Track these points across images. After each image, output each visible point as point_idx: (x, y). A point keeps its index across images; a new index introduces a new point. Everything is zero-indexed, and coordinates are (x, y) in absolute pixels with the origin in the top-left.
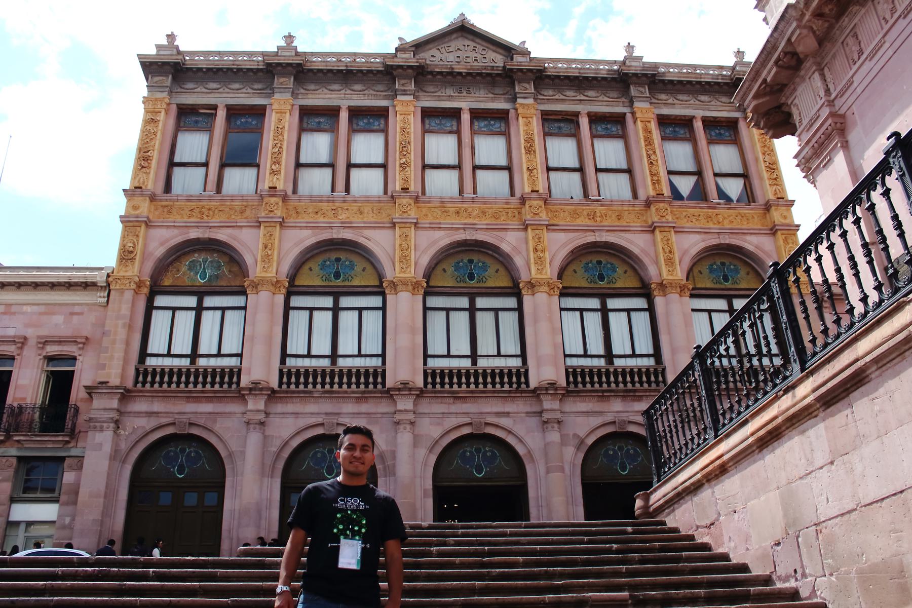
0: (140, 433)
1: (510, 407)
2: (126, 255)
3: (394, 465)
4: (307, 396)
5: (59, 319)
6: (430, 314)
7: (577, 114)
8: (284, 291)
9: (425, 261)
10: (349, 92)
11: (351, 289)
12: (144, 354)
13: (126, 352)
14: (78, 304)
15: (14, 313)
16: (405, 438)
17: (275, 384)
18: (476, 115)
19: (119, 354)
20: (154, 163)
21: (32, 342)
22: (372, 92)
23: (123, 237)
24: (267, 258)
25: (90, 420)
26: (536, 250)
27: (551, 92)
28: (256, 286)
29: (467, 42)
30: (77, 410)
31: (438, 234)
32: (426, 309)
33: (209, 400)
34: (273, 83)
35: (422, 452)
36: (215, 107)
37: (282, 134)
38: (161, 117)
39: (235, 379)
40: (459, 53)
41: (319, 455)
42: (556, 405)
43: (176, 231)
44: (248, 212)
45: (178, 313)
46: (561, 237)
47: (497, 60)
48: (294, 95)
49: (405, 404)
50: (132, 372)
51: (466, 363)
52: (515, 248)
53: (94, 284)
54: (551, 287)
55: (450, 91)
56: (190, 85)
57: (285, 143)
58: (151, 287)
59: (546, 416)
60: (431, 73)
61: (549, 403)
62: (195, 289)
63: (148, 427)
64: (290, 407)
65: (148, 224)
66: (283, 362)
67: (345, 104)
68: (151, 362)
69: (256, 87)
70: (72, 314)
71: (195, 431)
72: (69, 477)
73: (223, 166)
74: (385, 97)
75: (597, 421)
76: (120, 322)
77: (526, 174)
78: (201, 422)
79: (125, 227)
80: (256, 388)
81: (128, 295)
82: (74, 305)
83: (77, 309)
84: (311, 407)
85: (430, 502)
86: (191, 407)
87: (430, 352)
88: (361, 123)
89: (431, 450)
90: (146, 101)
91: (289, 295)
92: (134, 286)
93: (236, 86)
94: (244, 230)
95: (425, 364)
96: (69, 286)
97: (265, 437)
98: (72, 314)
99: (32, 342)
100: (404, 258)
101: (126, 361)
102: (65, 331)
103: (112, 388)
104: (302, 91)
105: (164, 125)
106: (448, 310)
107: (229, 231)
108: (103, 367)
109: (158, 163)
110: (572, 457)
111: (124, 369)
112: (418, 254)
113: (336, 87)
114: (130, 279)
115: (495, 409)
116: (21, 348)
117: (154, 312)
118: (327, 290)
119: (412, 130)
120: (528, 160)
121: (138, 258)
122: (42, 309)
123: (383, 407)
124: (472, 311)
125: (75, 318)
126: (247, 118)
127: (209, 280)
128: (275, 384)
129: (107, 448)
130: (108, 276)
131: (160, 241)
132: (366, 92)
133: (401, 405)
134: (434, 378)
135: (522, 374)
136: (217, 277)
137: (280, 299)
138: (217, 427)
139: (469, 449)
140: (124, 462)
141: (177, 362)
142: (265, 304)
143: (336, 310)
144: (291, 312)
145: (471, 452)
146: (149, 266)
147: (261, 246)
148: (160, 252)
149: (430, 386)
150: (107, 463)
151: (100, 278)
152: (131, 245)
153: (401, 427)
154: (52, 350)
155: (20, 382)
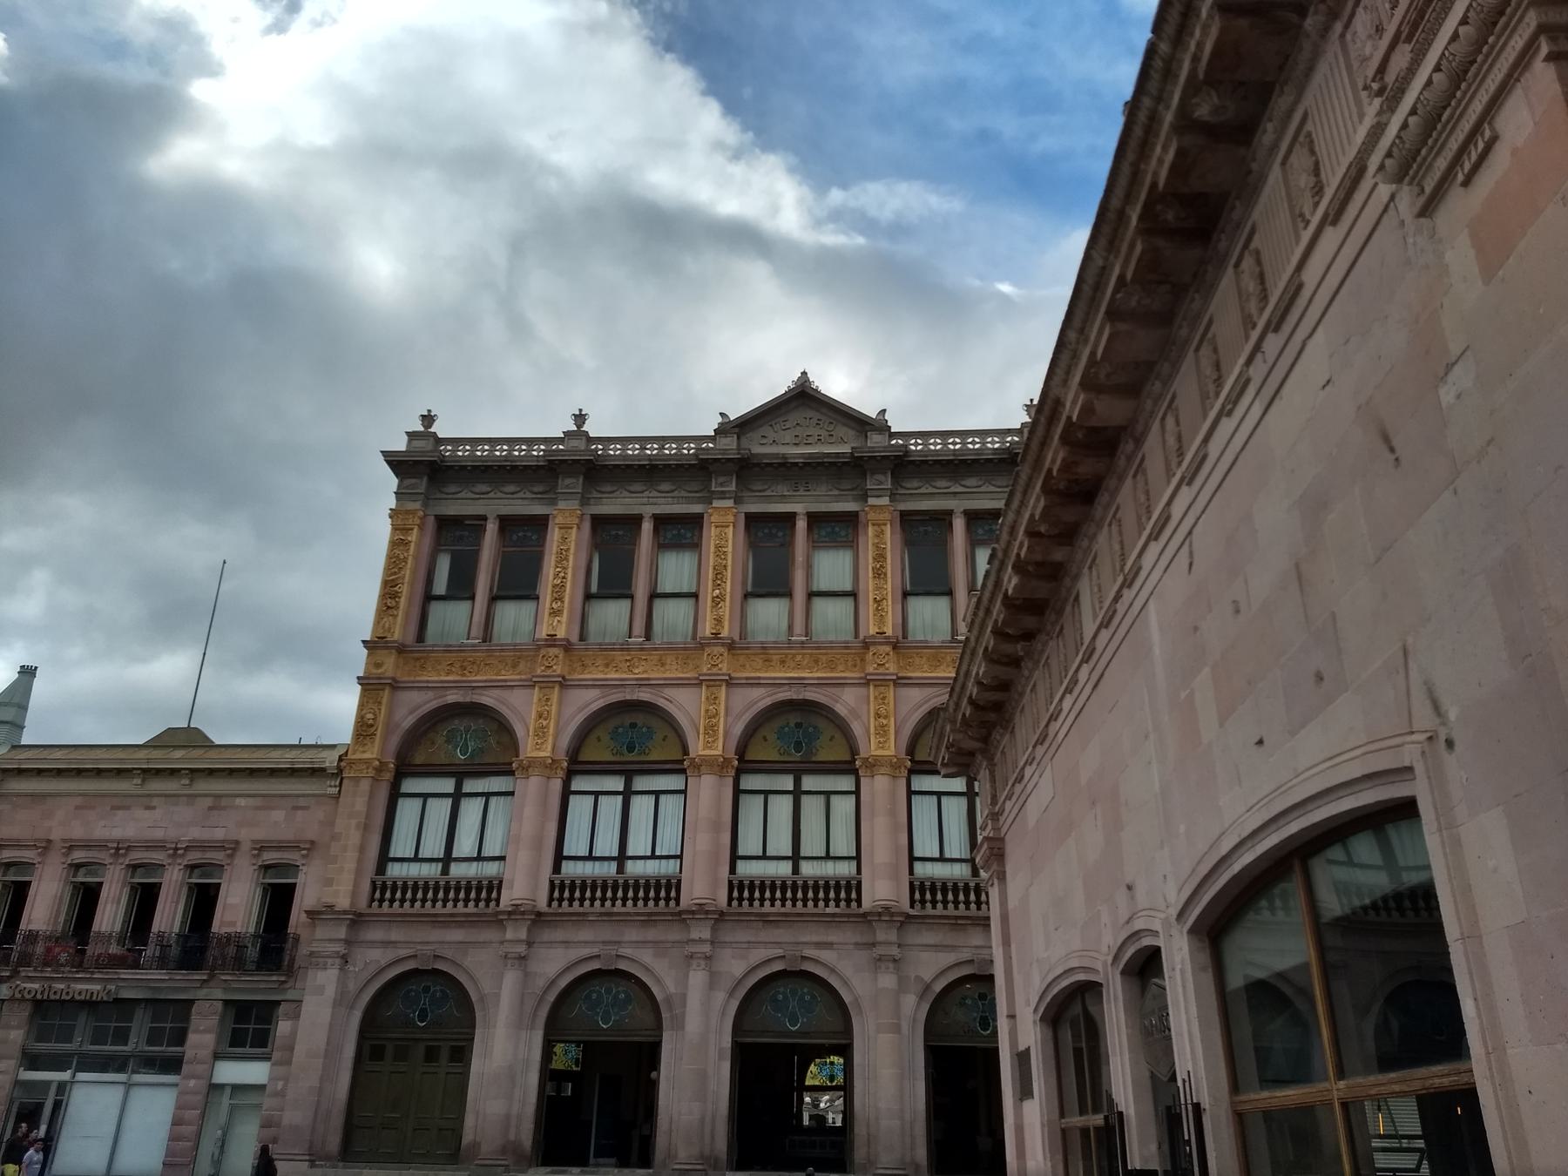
0: (372, 969)
1: (834, 936)
2: (363, 729)
3: (683, 1014)
4: (580, 919)
5: (278, 815)
6: (743, 799)
7: (950, 513)
8: (561, 774)
9: (738, 729)
10: (655, 494)
11: (646, 767)
12: (384, 859)
13: (360, 861)
15: (224, 808)
16: (697, 978)
17: (542, 904)
18: (814, 519)
19: (350, 865)
20: (403, 601)
21: (246, 846)
22: (684, 494)
23: (361, 706)
24: (541, 732)
25: (312, 953)
26: (878, 716)
27: (915, 484)
28: (526, 768)
29: (810, 413)
30: (297, 939)
31: (757, 693)
32: (738, 792)
33: (460, 925)
34: (556, 486)
35: (720, 996)
36: (484, 518)
37: (567, 559)
38: (413, 537)
39: (494, 895)
40: (798, 431)
41: (594, 996)
42: (893, 936)
43: (430, 694)
44: (522, 666)
45: (430, 801)
46: (915, 695)
47: (842, 446)
48: (585, 501)
49: (702, 931)
50: (366, 887)
51: (784, 869)
52: (852, 711)
53: (323, 770)
54: (896, 766)
55: (782, 489)
56: (452, 488)
57: (570, 571)
58: (397, 767)
59: (880, 950)
60: (758, 465)
61: (885, 934)
62: (453, 769)
63: (383, 963)
64: (559, 934)
65: (395, 686)
66: (557, 868)
67: (648, 511)
68: (395, 871)
69: (536, 489)
70: (296, 808)
71: (440, 966)
73: (494, 599)
74: (699, 501)
75: (949, 958)
76: (354, 822)
77: (872, 606)
78: (448, 953)
79: (364, 691)
80: (516, 912)
81: (365, 785)
82: (298, 796)
83: (302, 802)
84: (585, 934)
85: (726, 1066)
86: (436, 935)
87: (741, 852)
88: (669, 535)
89: (731, 994)
90: (394, 514)
91: (570, 774)
92: (372, 773)
93: (511, 488)
94: (516, 691)
95: (733, 870)
96: (293, 772)
97: (526, 974)
99: (246, 846)
100: (711, 729)
101: (359, 872)
102: (286, 834)
103: (339, 912)
104: (596, 495)
105: (418, 545)
106: (766, 793)
107: (496, 692)
108: (329, 882)
109: (410, 600)
110: (913, 1009)
111: (356, 885)
112: (730, 719)
113: (637, 487)
114: (367, 762)
115: (815, 938)
116: (231, 856)
117: (401, 801)
118: (617, 767)
119: (730, 549)
120: (878, 588)
121: (379, 733)
123: (674, 934)
124: (797, 794)
126: (525, 533)
127: (472, 756)
128: (542, 904)
129: (331, 991)
130: (340, 759)
131: (411, 706)
132: (676, 494)
133: (695, 935)
134: (741, 892)
135: (850, 889)
136: (482, 750)
137: (557, 785)
138: (468, 962)
139: (781, 990)
140: (352, 1007)
142: (534, 791)
143: (627, 794)
144: (573, 799)
145: (786, 998)
146: (395, 741)
147: (533, 715)
148: (408, 722)
149: (735, 903)
150: (329, 1011)
151: (330, 760)
152: (370, 716)
153: (695, 963)
154: (270, 857)
155: (231, 900)
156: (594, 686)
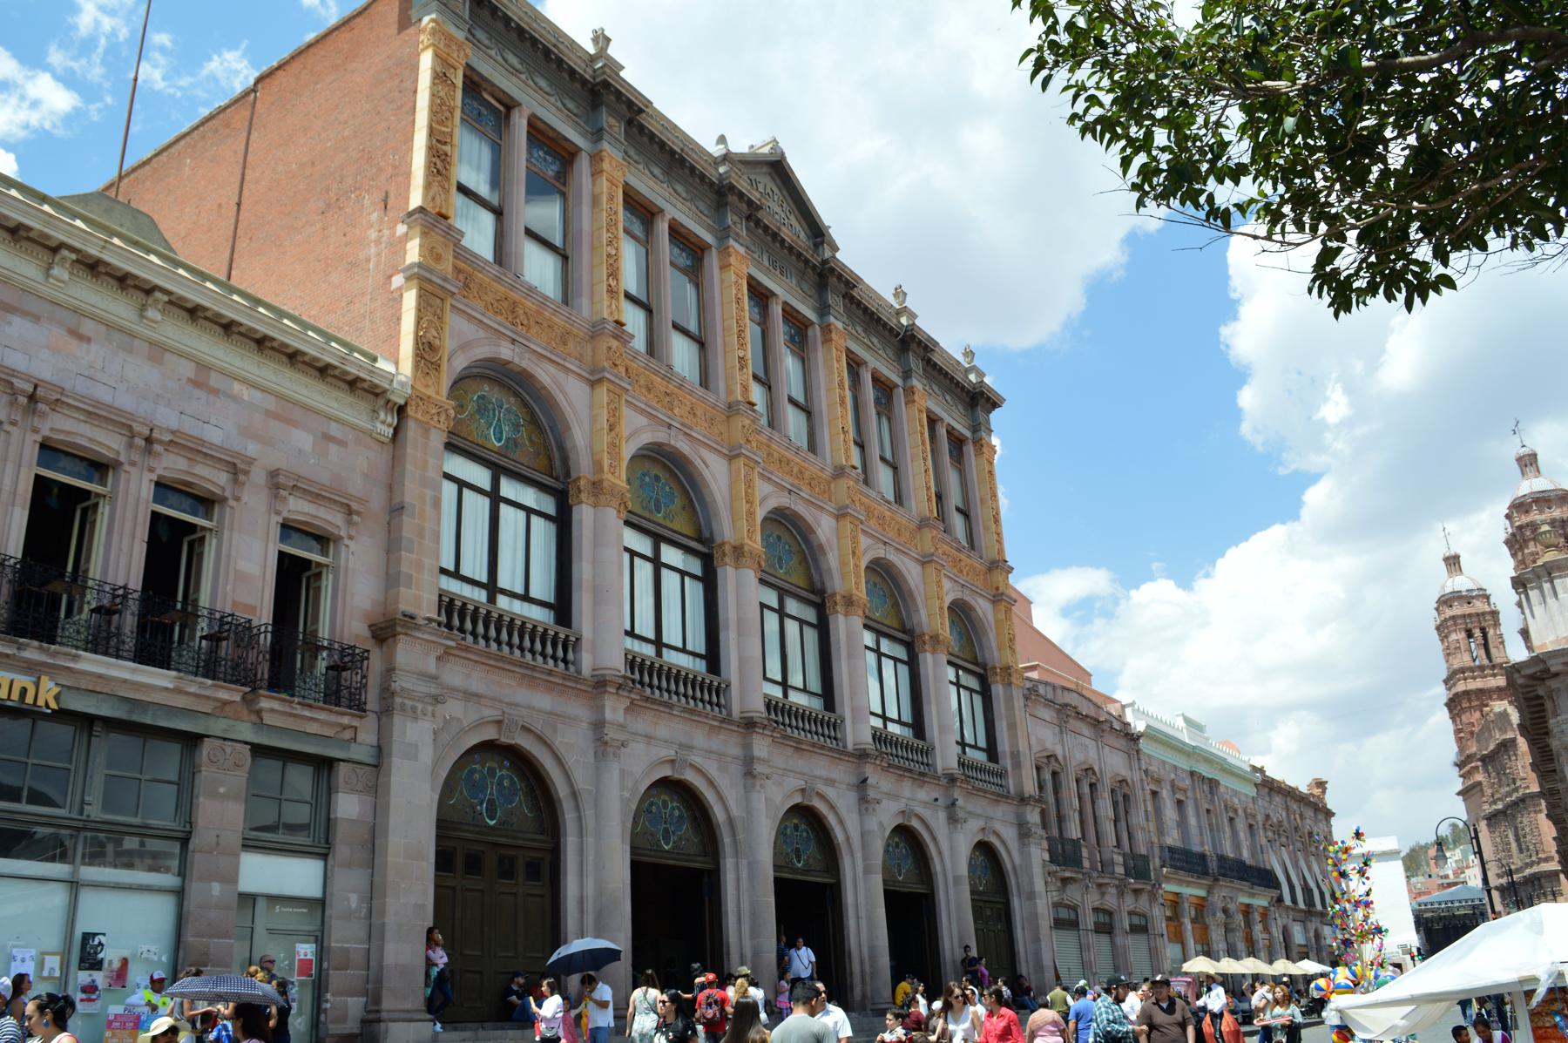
5: (303, 440)
14: (338, 421)
15: (215, 392)
21: (258, 477)
72: (348, 806)
82: (329, 418)
83: (335, 430)
98: (328, 438)
99: (258, 477)
107: (552, 369)
122: (270, 403)
125: (333, 448)
141: (467, 591)
154: (299, 508)
156: (643, 412)
